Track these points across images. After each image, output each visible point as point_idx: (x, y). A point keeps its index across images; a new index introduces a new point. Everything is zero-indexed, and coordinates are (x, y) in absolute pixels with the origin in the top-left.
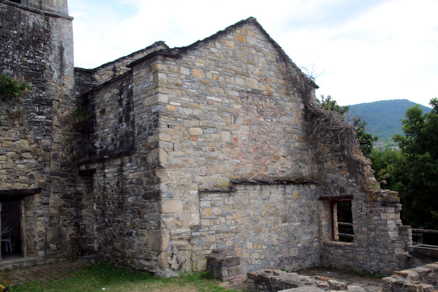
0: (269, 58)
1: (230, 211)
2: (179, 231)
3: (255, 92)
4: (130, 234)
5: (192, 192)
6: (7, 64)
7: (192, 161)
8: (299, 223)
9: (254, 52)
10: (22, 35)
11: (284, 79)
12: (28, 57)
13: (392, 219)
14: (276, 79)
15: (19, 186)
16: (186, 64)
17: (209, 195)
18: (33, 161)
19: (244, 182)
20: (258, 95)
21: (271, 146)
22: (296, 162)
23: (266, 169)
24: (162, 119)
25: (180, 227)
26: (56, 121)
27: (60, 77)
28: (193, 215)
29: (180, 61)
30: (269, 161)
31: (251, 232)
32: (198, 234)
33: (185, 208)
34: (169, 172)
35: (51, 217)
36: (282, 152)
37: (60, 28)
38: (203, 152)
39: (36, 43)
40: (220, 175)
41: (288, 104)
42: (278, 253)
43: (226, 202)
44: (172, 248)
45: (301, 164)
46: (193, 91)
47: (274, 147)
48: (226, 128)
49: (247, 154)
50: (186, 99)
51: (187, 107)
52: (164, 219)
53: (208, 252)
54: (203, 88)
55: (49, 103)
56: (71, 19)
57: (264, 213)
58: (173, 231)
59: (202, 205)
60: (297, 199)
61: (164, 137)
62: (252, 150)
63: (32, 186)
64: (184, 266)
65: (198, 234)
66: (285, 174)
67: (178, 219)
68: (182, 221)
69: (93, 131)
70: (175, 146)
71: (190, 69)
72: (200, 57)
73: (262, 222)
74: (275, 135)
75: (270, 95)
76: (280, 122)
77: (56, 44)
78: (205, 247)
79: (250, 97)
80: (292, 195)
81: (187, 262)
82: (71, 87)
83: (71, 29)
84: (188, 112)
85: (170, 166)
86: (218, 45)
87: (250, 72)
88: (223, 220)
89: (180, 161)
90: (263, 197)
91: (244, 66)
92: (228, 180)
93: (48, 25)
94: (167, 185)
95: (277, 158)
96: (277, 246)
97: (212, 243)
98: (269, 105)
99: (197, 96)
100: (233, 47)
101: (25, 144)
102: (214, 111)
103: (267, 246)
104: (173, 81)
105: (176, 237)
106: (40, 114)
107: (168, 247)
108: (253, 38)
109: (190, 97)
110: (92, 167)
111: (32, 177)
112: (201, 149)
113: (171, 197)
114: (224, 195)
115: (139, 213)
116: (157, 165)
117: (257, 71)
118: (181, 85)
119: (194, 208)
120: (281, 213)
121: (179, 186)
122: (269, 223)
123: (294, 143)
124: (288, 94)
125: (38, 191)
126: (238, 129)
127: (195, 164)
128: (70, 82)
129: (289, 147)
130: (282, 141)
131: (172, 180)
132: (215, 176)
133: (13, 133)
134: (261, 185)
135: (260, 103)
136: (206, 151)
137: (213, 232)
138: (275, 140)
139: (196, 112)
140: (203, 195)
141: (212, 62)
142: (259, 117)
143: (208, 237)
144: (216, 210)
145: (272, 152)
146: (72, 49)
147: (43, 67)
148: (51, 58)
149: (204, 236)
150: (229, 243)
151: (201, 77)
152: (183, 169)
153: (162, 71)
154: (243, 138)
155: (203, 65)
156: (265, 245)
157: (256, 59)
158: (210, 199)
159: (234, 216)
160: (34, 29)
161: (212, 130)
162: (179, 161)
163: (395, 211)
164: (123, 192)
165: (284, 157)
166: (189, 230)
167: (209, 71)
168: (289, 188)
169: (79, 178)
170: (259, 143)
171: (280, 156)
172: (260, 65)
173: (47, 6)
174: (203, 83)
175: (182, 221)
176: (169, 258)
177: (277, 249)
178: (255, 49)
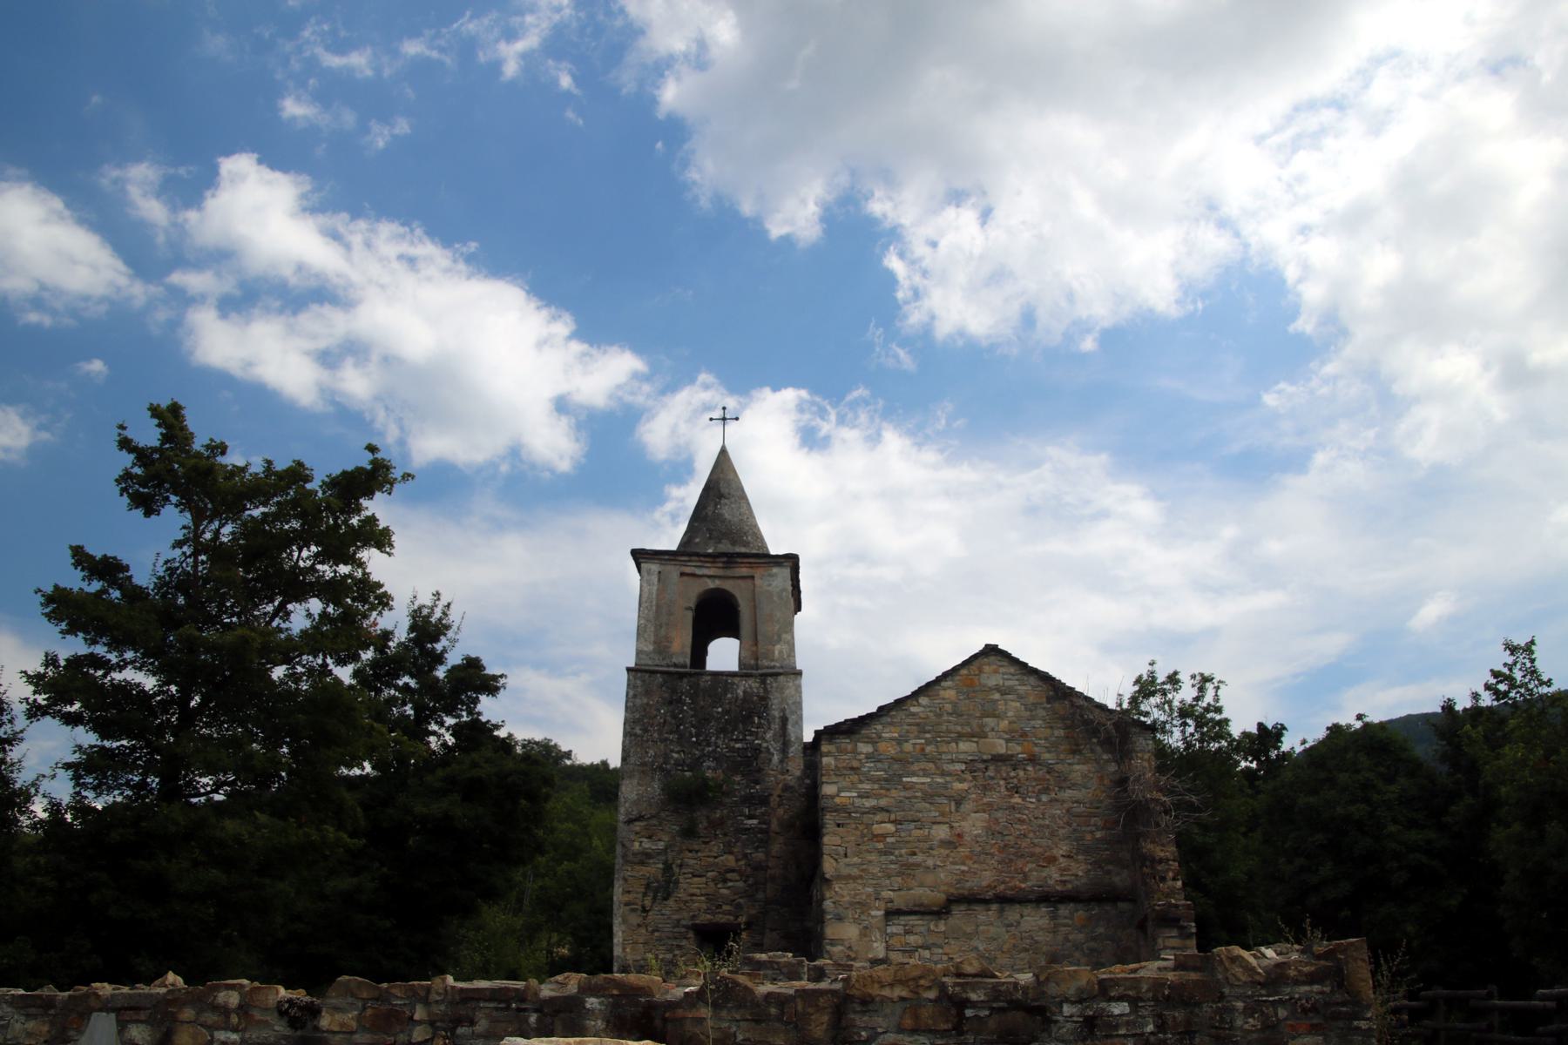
0: (1031, 699)
1: (940, 941)
3: (998, 759)
6: (709, 755)
7: (876, 870)
9: (997, 696)
10: (727, 712)
11: (1067, 727)
12: (737, 741)
15: (722, 919)
18: (740, 884)
19: (972, 900)
22: (1097, 864)
23: (1026, 878)
25: (854, 959)
26: (774, 826)
27: (781, 761)
30: (1030, 866)
36: (1063, 848)
37: (781, 689)
39: (747, 719)
45: (1110, 867)
47: (1044, 842)
48: (940, 819)
50: (867, 786)
55: (764, 800)
56: (799, 673)
57: (1006, 947)
61: (829, 840)
66: (1069, 886)
67: (850, 948)
71: (874, 743)
72: (891, 724)
77: (776, 714)
79: (992, 768)
80: (1072, 918)
82: (798, 773)
83: (798, 689)
84: (869, 803)
85: (839, 877)
88: (926, 954)
91: (974, 723)
92: (943, 897)
93: (765, 689)
99: (886, 780)
101: (730, 860)
106: (750, 817)
108: (993, 677)
111: (739, 906)
113: (840, 918)
117: (1004, 724)
120: (1045, 949)
121: (852, 904)
124: (1074, 752)
126: (964, 819)
128: (796, 767)
129: (1077, 840)
130: (1062, 832)
133: (716, 847)
139: (883, 802)
142: (1011, 797)
144: (912, 939)
145: (1038, 850)
146: (801, 717)
147: (757, 749)
148: (769, 736)
153: (828, 754)
157: (1001, 707)
159: (947, 949)
160: (744, 700)
161: (912, 826)
162: (855, 872)
166: (867, 965)
168: (1064, 910)
172: (1010, 714)
173: (766, 663)
174: (895, 760)
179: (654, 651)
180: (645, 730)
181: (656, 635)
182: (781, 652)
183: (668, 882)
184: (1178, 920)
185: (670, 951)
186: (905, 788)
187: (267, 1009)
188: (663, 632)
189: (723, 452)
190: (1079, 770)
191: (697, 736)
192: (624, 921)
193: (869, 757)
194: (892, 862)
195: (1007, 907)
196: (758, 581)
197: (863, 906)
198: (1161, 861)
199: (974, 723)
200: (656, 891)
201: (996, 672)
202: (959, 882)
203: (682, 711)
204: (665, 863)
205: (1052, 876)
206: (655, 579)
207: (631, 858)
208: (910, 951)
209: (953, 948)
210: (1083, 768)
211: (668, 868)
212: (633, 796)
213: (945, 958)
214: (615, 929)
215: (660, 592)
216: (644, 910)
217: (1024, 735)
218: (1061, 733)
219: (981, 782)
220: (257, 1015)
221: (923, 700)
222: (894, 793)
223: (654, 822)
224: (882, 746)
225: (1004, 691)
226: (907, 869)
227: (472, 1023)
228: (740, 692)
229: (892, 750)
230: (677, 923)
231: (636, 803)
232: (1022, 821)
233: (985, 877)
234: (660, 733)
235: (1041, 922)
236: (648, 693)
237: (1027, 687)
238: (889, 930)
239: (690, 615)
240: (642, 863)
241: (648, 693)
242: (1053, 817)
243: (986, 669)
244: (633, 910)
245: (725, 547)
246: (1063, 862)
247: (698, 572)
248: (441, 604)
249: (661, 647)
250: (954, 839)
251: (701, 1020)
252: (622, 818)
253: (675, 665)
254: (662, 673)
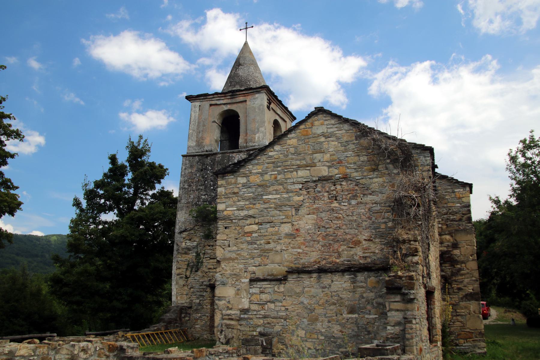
0: (345, 139)
1: (280, 298)
2: (229, 312)
3: (323, 179)
5: (243, 280)
7: (245, 254)
8: (377, 316)
9: (322, 139)
13: (398, 310)
14: (357, 158)
16: (243, 174)
17: (258, 283)
20: (329, 181)
21: (347, 231)
23: (339, 256)
24: (219, 223)
25: (231, 309)
28: (243, 300)
29: (238, 173)
31: (305, 320)
32: (246, 316)
33: (237, 294)
34: (223, 265)
36: (364, 235)
38: (258, 245)
40: (276, 265)
41: (375, 180)
42: (340, 346)
43: (276, 289)
44: (222, 325)
46: (249, 195)
47: (352, 231)
49: (312, 243)
50: (242, 203)
51: (242, 210)
52: (217, 302)
53: (255, 333)
54: (260, 190)
57: (321, 302)
58: (224, 312)
59: (251, 292)
60: (374, 287)
62: (320, 238)
64: (232, 342)
65: (246, 316)
66: (369, 260)
67: (229, 302)
68: (232, 305)
70: (231, 243)
71: (247, 177)
73: (319, 311)
74: (355, 218)
76: (361, 203)
78: (252, 329)
80: (366, 283)
81: (234, 340)
85: (225, 259)
87: (316, 161)
88: (272, 306)
89: (234, 254)
90: (322, 285)
91: (308, 158)
94: (221, 275)
95: (358, 243)
96: (339, 338)
97: (259, 326)
98: (346, 188)
99: (253, 198)
100: (296, 145)
102: (271, 208)
103: (326, 337)
104: (230, 191)
105: (227, 317)
107: (219, 325)
109: (247, 200)
112: (256, 244)
113: (224, 284)
114: (274, 283)
117: (327, 157)
118: (237, 193)
121: (231, 275)
122: (329, 312)
123: (385, 223)
124: (374, 170)
126: (300, 220)
127: (247, 257)
129: (375, 229)
130: (365, 223)
131: (226, 270)
132: (272, 266)
134: (319, 273)
135: (333, 188)
136: (261, 244)
137: (261, 316)
138: (355, 225)
139: (251, 212)
140: (252, 283)
141: (270, 165)
143: (255, 320)
144: (264, 297)
145: (348, 237)
149: (251, 319)
150: (278, 328)
151: (258, 181)
152: (236, 261)
154: (308, 227)
155: (260, 170)
156: (322, 335)
157: (325, 146)
158: (259, 286)
159: (284, 303)
162: (234, 255)
163: (403, 300)
165: (369, 240)
166: (238, 312)
167: (266, 174)
168: (360, 277)
170: (330, 229)
171: (362, 240)
172: (331, 150)
173: (251, 144)
174: (260, 186)
175: (232, 305)
176: (219, 333)
177: (339, 341)
178: (324, 136)
179: (196, 146)
180: (190, 186)
181: (197, 137)
182: (259, 138)
183: (198, 262)
184: (400, 289)
185: (198, 298)
186: (265, 203)
188: (200, 135)
189: (246, 44)
190: (376, 181)
192: (177, 283)
193: (244, 185)
194: (255, 249)
195: (323, 275)
196: (248, 103)
197: (237, 276)
198: (404, 242)
199: (308, 158)
200: (192, 268)
201: (322, 124)
202: (296, 259)
203: (207, 174)
204: (197, 253)
205: (358, 255)
206: (197, 109)
207: (181, 251)
208: (262, 304)
209: (288, 302)
210: (380, 180)
211: (198, 255)
212: (183, 220)
213: (283, 309)
215: (200, 116)
216: (187, 277)
217: (340, 162)
218: (365, 158)
219: (312, 194)
221: (277, 147)
222: (258, 206)
223: (192, 232)
224: (252, 178)
225: (326, 136)
226: (264, 253)
231: (184, 223)
232: (338, 218)
233: (312, 257)
234: (197, 187)
235: (344, 285)
236: (191, 167)
237: (344, 132)
238: (252, 291)
240: (186, 253)
241: (191, 167)
242: (359, 214)
243: (316, 123)
244: (181, 278)
246: (365, 244)
247: (218, 102)
248: (142, 141)
249: (199, 144)
250: (294, 232)
252: (177, 231)
253: (207, 151)
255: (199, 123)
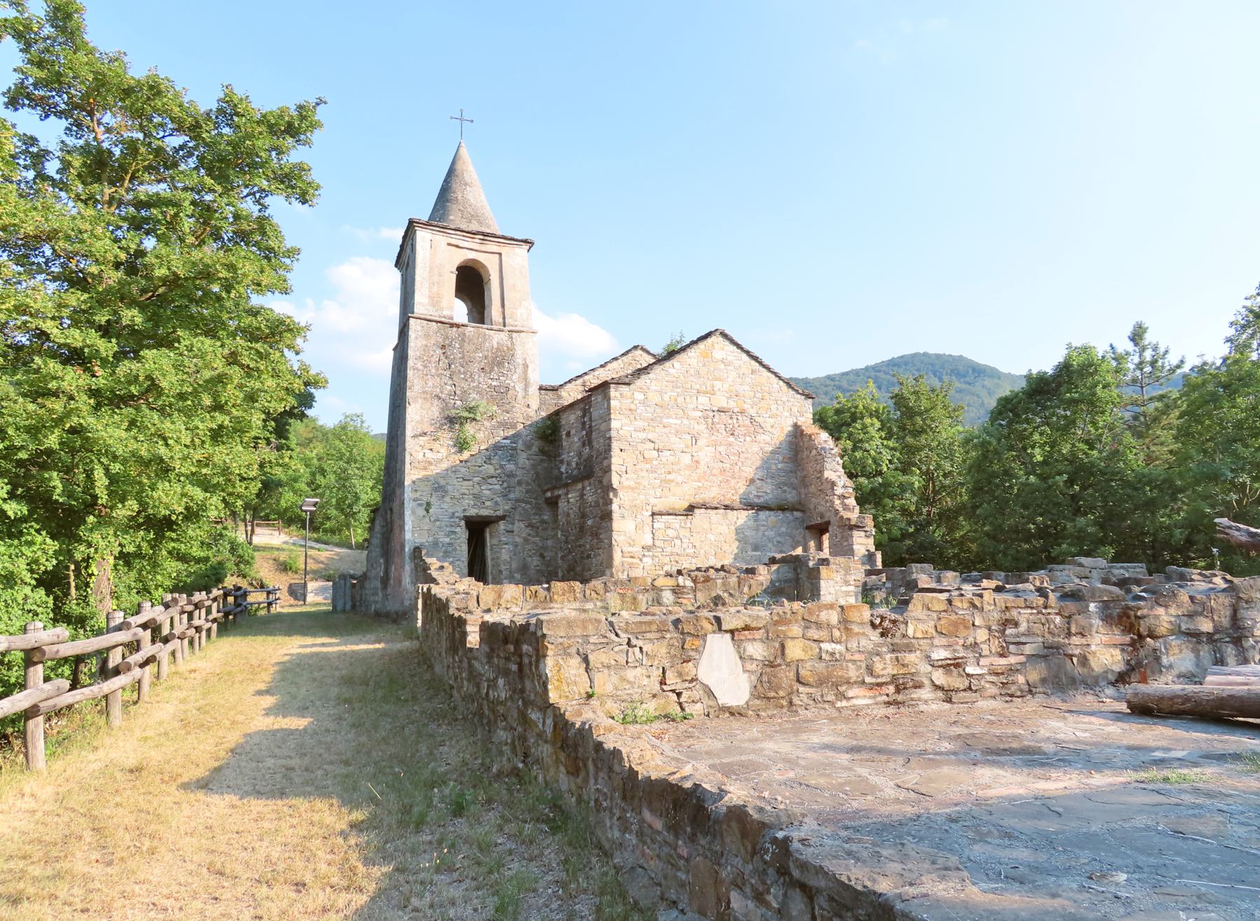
2: (630, 549)
4: (589, 556)
7: (646, 483)
9: (722, 366)
10: (486, 358)
18: (498, 487)
19: (705, 506)
22: (779, 486)
34: (620, 494)
35: (516, 546)
39: (500, 364)
50: (640, 424)
54: (658, 410)
61: (616, 460)
63: (498, 513)
69: (559, 455)
75: (742, 412)
77: (520, 361)
84: (642, 435)
86: (677, 364)
91: (709, 384)
92: (686, 505)
93: (512, 343)
110: (556, 493)
111: (496, 503)
115: (596, 535)
116: (609, 487)
117: (726, 386)
119: (648, 529)
125: (503, 518)
139: (651, 436)
144: (671, 533)
148: (515, 377)
162: (632, 484)
164: (584, 516)
168: (763, 515)
169: (544, 506)
180: (425, 367)
187: (862, 624)
188: (435, 289)
191: (464, 373)
192: (413, 513)
199: (709, 384)
214: (407, 518)
220: (856, 629)
227: (1016, 624)
228: (495, 345)
229: (657, 399)
230: (453, 515)
231: (421, 422)
236: (427, 336)
239: (454, 277)
244: (420, 505)
245: (474, 227)
251: (1157, 617)
254: (437, 322)
255: (431, 269)
